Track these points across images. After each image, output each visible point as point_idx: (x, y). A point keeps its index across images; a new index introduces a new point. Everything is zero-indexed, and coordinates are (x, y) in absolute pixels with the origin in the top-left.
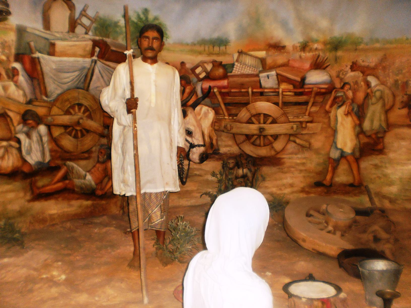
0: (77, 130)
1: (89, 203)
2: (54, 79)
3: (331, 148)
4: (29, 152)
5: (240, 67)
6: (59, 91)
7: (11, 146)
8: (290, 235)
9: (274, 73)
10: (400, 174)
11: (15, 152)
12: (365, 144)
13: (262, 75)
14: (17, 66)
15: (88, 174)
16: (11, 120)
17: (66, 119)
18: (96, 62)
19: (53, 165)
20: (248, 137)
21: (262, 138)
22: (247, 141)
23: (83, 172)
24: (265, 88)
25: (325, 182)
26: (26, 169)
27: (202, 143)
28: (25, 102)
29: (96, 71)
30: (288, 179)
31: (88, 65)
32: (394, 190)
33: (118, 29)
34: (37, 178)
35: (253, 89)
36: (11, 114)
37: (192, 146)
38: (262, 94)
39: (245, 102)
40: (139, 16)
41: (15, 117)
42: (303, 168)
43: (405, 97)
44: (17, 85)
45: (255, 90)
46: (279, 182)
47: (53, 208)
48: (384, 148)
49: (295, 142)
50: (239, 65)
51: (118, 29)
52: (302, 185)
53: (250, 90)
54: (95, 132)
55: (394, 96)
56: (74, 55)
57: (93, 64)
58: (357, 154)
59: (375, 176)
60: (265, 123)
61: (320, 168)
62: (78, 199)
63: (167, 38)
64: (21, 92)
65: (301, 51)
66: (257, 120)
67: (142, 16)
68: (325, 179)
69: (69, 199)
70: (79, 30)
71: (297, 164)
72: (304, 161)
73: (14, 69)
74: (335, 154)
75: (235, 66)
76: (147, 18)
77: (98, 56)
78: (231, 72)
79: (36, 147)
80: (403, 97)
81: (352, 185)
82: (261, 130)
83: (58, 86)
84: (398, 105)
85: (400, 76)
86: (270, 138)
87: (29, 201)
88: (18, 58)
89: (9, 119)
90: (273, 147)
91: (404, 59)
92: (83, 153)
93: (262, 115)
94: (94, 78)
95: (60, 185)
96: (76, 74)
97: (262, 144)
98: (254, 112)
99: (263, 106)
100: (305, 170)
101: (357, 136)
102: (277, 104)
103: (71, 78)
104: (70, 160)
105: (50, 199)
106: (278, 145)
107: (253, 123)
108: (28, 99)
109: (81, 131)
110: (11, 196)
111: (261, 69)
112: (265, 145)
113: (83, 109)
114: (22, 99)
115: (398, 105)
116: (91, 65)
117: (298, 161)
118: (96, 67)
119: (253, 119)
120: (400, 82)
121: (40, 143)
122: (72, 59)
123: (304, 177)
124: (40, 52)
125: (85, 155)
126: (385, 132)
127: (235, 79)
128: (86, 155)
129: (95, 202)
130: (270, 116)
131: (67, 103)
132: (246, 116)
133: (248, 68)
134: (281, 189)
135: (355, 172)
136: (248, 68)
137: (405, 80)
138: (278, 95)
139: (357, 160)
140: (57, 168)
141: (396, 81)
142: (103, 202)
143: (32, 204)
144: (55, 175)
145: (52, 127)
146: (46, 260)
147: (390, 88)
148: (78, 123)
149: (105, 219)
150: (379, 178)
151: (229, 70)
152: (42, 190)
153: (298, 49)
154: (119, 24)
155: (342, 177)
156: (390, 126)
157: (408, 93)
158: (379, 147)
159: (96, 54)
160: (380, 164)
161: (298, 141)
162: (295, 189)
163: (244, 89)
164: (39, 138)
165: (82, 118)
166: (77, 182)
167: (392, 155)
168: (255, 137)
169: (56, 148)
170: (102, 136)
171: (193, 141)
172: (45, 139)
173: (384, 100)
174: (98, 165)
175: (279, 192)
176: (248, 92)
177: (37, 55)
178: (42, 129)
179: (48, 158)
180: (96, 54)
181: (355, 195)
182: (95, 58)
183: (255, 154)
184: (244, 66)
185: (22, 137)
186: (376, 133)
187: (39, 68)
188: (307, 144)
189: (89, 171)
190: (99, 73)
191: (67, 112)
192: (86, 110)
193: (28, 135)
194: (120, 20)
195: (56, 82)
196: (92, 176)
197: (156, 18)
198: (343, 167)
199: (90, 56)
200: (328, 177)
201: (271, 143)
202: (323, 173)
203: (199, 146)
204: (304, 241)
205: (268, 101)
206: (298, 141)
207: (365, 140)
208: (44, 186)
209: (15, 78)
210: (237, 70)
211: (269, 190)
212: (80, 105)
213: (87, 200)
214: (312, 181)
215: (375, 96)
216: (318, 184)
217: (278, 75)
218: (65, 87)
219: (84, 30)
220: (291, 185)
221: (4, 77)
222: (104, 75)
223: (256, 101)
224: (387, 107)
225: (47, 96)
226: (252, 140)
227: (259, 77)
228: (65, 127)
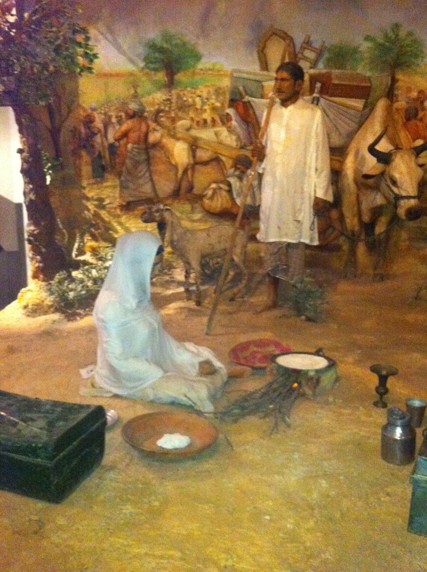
7: (220, 188)
11: (224, 193)
14: (231, 111)
16: (224, 164)
27: (412, 194)
28: (239, 147)
36: (223, 158)
37: (398, 198)
40: (386, 36)
41: (228, 163)
44: (230, 130)
63: (423, 57)
64: (234, 137)
67: (391, 34)
73: (228, 114)
88: (233, 103)
89: (222, 164)
108: (242, 144)
114: (234, 144)
124: (251, 96)
159: (316, 90)
171: (400, 192)
177: (247, 98)
185: (233, 180)
187: (251, 112)
193: (240, 178)
194: (361, 44)
197: (410, 34)
199: (308, 93)
203: (409, 197)
209: (229, 124)
221: (218, 123)
222: (329, 113)
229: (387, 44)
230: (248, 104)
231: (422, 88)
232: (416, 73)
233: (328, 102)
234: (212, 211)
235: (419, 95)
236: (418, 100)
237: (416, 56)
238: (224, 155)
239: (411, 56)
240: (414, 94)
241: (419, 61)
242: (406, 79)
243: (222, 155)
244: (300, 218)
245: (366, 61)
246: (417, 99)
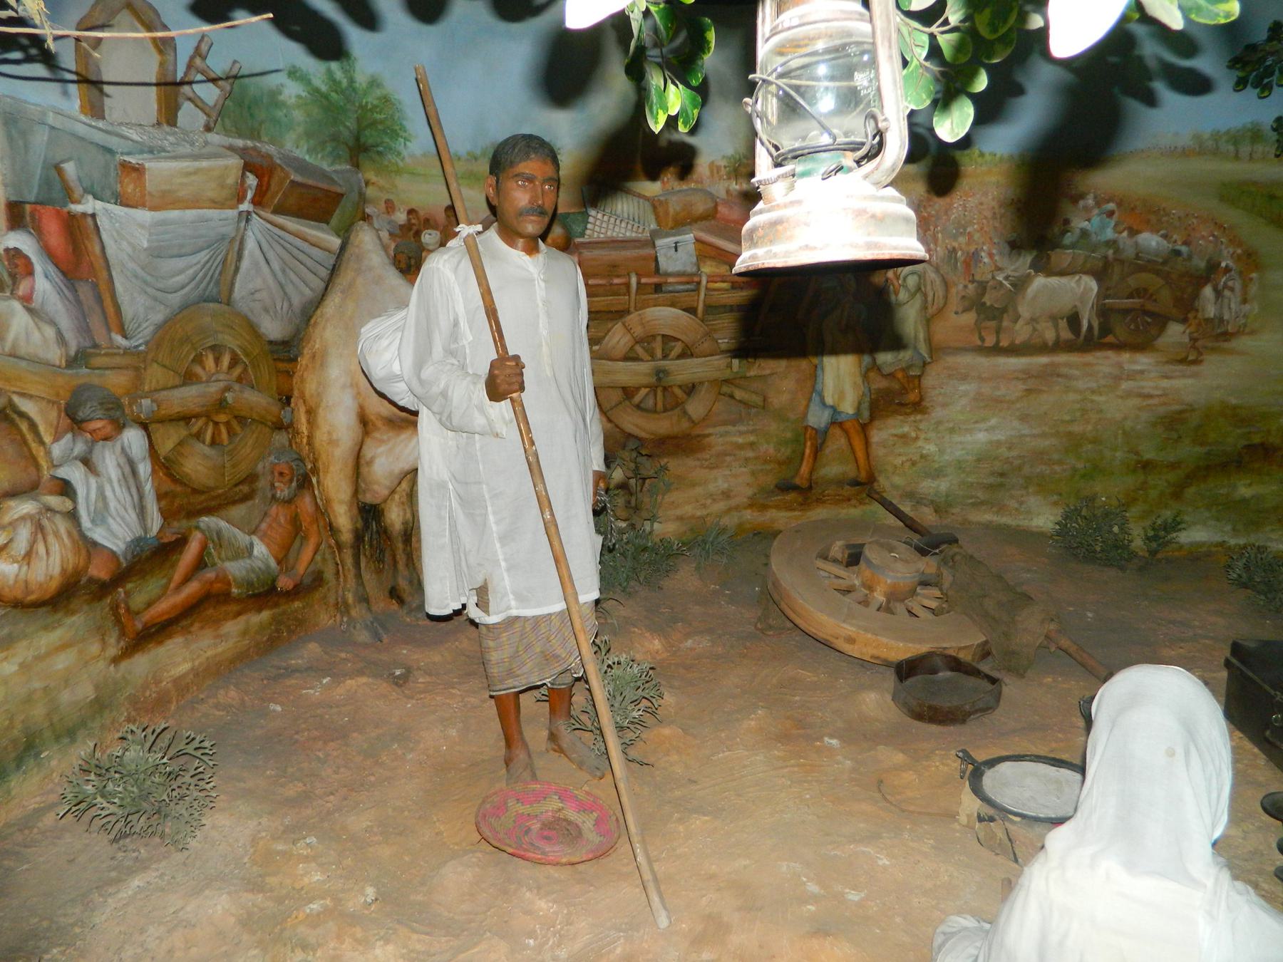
0: (216, 424)
1: (266, 615)
2: (145, 282)
3: (807, 406)
4: (100, 517)
5: (602, 222)
6: (158, 317)
8: (812, 630)
9: (690, 237)
10: (958, 453)
11: (62, 525)
12: (879, 390)
13: (659, 242)
15: (255, 540)
16: (33, 426)
17: (188, 397)
18: (247, 216)
19: (169, 537)
20: (628, 392)
21: (659, 393)
22: (627, 403)
23: (242, 538)
24: (668, 275)
25: (797, 481)
26: (99, 571)
29: (250, 245)
30: (719, 481)
31: (229, 230)
33: (280, 114)
34: (129, 586)
35: (639, 276)
38: (658, 288)
39: (620, 308)
42: (750, 454)
43: (971, 286)
45: (644, 280)
46: (699, 490)
47: (178, 657)
48: (922, 399)
49: (732, 396)
50: (599, 216)
51: (280, 114)
52: (750, 492)
53: (634, 280)
54: (262, 422)
55: (946, 285)
56: (193, 203)
57: (243, 224)
58: (866, 414)
60: (665, 357)
61: (786, 452)
62: (239, 614)
64: (50, 332)
65: (729, 178)
66: (646, 350)
69: (217, 622)
70: (189, 115)
71: (741, 447)
72: (752, 438)
74: (817, 418)
75: (591, 219)
76: (352, 81)
77: (254, 202)
78: (583, 235)
79: (118, 496)
80: (966, 287)
81: (855, 483)
82: (660, 373)
83: (155, 299)
84: (955, 303)
85: (962, 240)
86: (678, 391)
87: (116, 660)
89: (24, 427)
90: (685, 413)
91: (972, 202)
92: (236, 485)
93: (659, 339)
94: (245, 264)
95: (193, 588)
96: (203, 256)
97: (660, 406)
98: (639, 331)
99: (663, 316)
100: (756, 458)
101: (865, 376)
102: (691, 310)
103: (191, 271)
104: (209, 511)
105: (170, 637)
106: (696, 408)
107: (636, 359)
109: (227, 424)
110: (62, 662)
111: (653, 226)
112: (665, 410)
113: (226, 361)
114: (55, 355)
115: (955, 303)
116: (238, 229)
117: (740, 440)
118: (249, 233)
119: (639, 349)
120: (959, 253)
121: (131, 481)
122: (191, 214)
123: (753, 473)
125: (240, 491)
126: (925, 364)
127: (597, 253)
128: (245, 489)
129: (276, 611)
130: (676, 339)
131: (186, 348)
132: (622, 342)
133: (623, 225)
134: (704, 506)
135: (860, 454)
136: (623, 225)
137: (972, 249)
138: (697, 290)
139: (864, 428)
140: (182, 542)
141: (954, 250)
142: (297, 604)
143: (124, 665)
144: (173, 566)
145: (152, 427)
146: (254, 841)
147: (937, 269)
148: (221, 404)
149: (312, 650)
150: (914, 464)
151: (577, 228)
152: (146, 617)
153: (723, 172)
154: (281, 98)
155: (833, 468)
156: (936, 350)
157: (977, 278)
158: (912, 397)
160: (913, 435)
161: (739, 394)
162: (733, 502)
163: (618, 276)
164: (127, 469)
165: (228, 389)
166: (236, 569)
167: (938, 413)
168: (643, 392)
169: (168, 486)
170: (279, 426)
172: (144, 469)
173: (925, 295)
174: (274, 509)
176: (628, 285)
177: (88, 205)
178: (133, 438)
179: (155, 522)
180: (250, 195)
181: (861, 503)
182: (246, 206)
183: (644, 430)
184: (612, 220)
185: (75, 474)
186: (910, 367)
188: (757, 399)
189: (253, 533)
190: (258, 252)
191: (189, 378)
192: (235, 361)
195: (149, 290)
196: (268, 545)
197: (374, 83)
198: (837, 442)
200: (805, 469)
201: (678, 404)
202: (793, 461)
204: (851, 640)
205: (673, 305)
206: (739, 394)
207: (882, 384)
208: (149, 605)
209: (23, 288)
210: (597, 229)
211: (679, 512)
212: (217, 350)
213: (260, 610)
214: (770, 481)
215: (905, 287)
216: (785, 487)
217: (698, 240)
218: (176, 299)
219: (202, 119)
220: (726, 495)
222: (271, 255)
223: (645, 305)
224: (931, 311)
225: (125, 337)
226: (637, 399)
227: (654, 246)
228: (186, 419)
229: (333, 94)
230: (89, 220)
231: (414, 206)
232: (399, 172)
233: (269, 226)
235: (409, 220)
236: (410, 230)
237: (394, 135)
238: (31, 397)
239: (384, 131)
240: (401, 217)
241: (399, 144)
242: (381, 181)
243: (23, 395)
245: (300, 130)
246: (406, 228)
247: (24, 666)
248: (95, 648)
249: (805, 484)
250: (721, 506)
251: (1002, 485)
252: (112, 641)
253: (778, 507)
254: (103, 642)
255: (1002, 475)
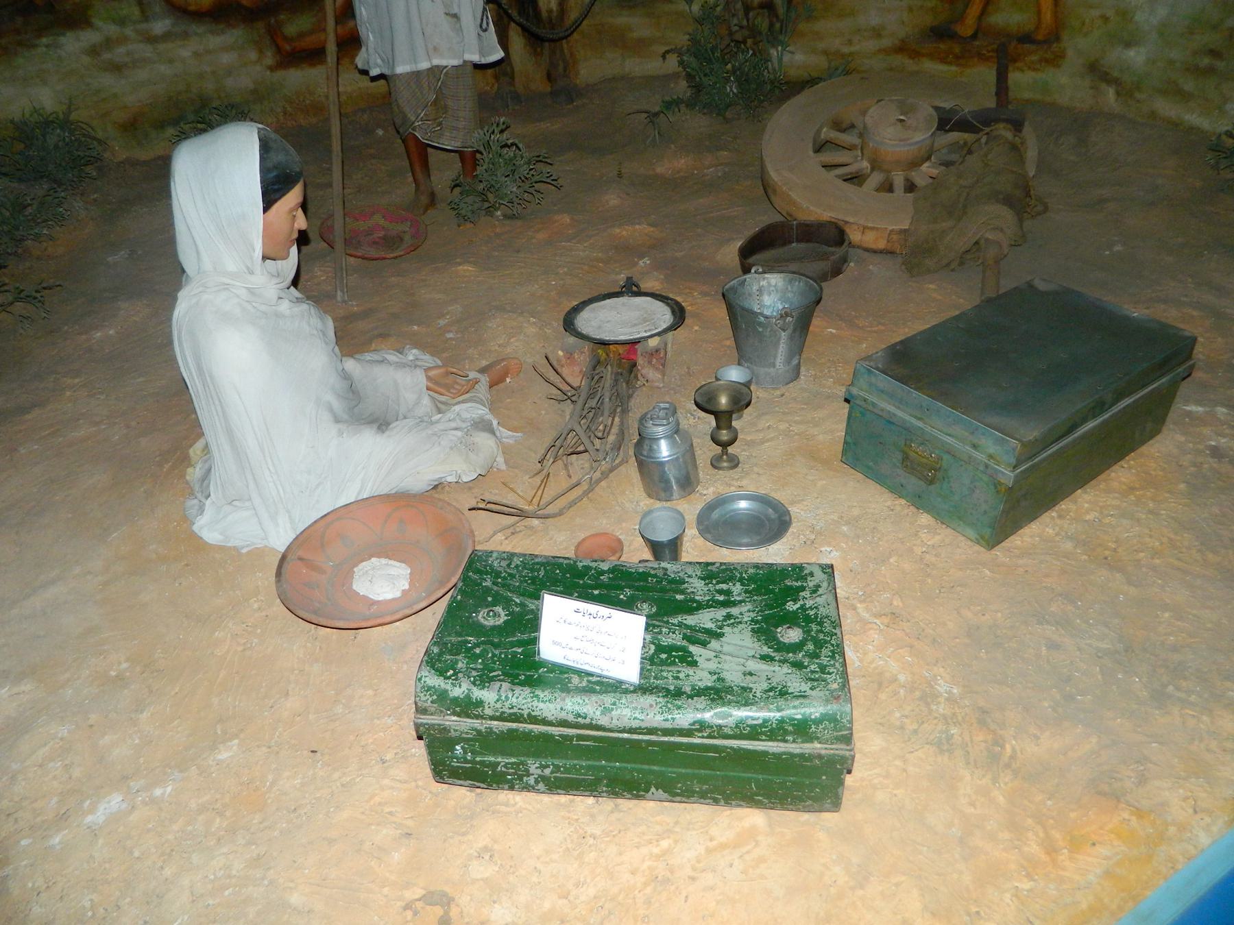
32: (1136, 57)
59: (1095, 13)
68: (961, 18)
87: (272, 69)
110: (226, 59)
143: (280, 74)
162: (886, 42)
175: (846, 50)
208: (301, 35)
211: (821, 46)
214: (929, 20)
216: (941, 33)
220: (877, 33)
234: (192, 8)
244: (456, 10)
247: (196, 54)
248: (253, 55)
249: (970, 32)
250: (871, 45)
251: (1210, 70)
252: (269, 54)
253: (931, 56)
254: (261, 51)
255: (1214, 53)
